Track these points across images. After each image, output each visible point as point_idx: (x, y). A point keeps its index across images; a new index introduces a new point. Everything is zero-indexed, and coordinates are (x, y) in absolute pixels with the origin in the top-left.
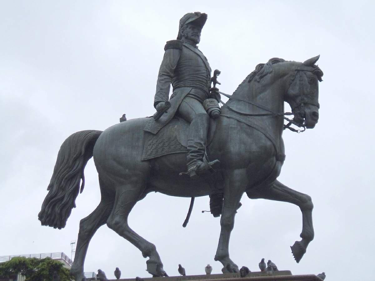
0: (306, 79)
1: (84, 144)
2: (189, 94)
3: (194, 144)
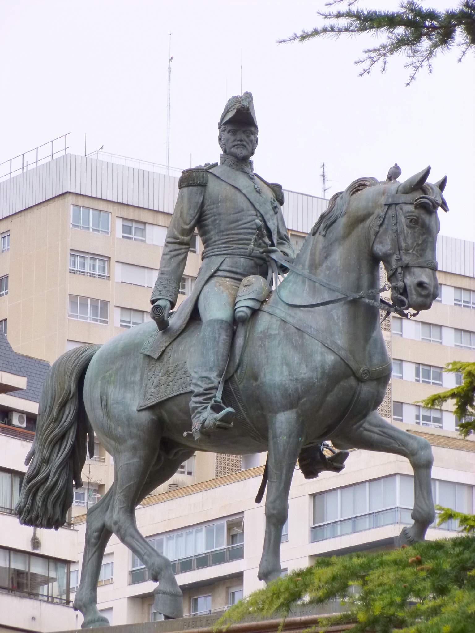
0: (403, 219)
1: (73, 377)
2: (218, 270)
3: (198, 380)
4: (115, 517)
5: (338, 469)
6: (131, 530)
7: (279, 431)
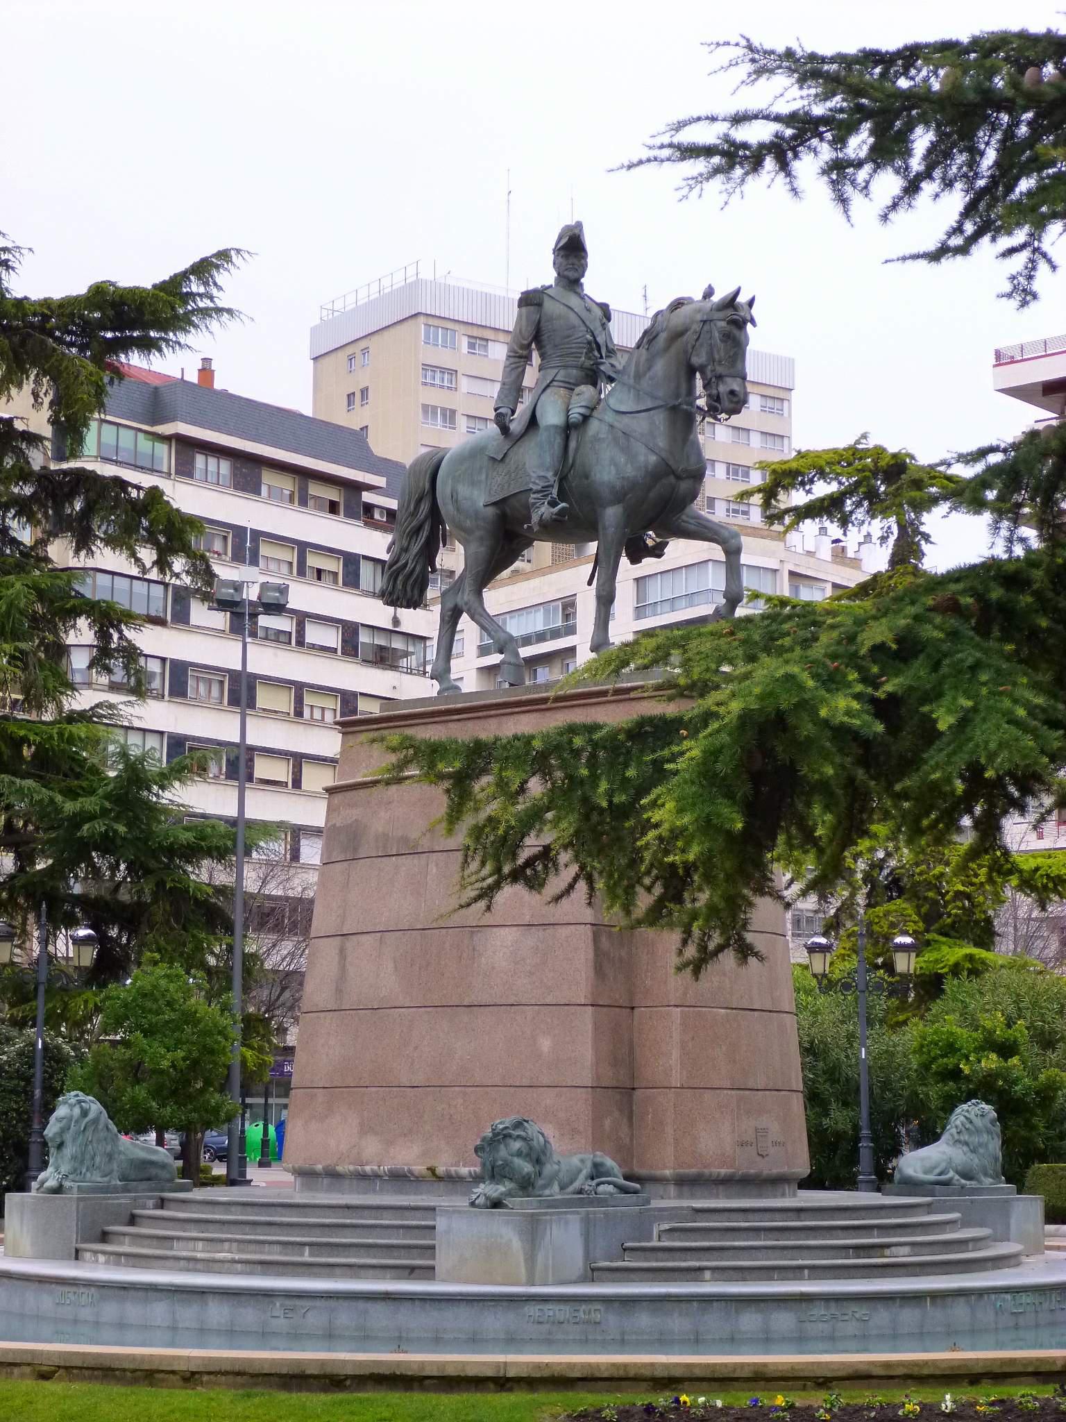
0: (717, 334)
2: (553, 380)
4: (466, 598)
5: (659, 556)
6: (480, 610)
7: (607, 523)
